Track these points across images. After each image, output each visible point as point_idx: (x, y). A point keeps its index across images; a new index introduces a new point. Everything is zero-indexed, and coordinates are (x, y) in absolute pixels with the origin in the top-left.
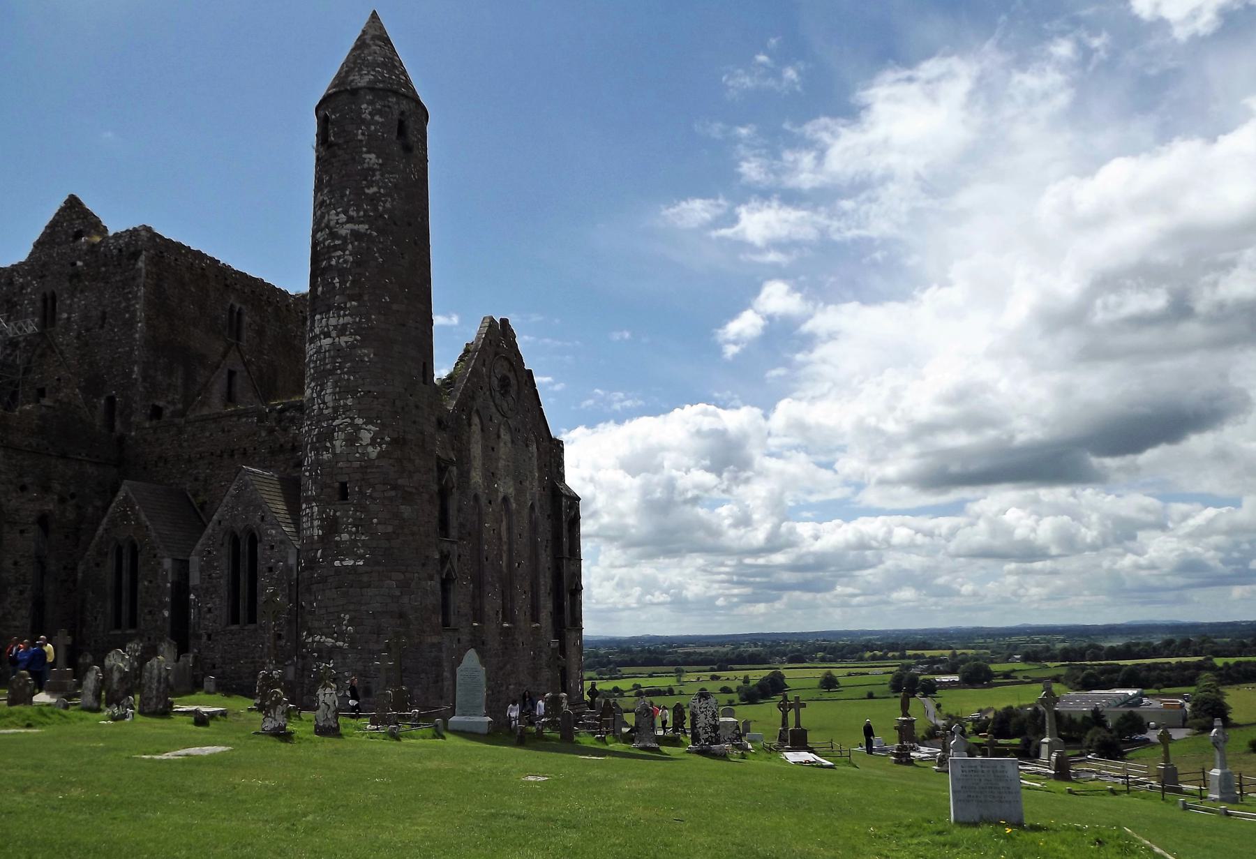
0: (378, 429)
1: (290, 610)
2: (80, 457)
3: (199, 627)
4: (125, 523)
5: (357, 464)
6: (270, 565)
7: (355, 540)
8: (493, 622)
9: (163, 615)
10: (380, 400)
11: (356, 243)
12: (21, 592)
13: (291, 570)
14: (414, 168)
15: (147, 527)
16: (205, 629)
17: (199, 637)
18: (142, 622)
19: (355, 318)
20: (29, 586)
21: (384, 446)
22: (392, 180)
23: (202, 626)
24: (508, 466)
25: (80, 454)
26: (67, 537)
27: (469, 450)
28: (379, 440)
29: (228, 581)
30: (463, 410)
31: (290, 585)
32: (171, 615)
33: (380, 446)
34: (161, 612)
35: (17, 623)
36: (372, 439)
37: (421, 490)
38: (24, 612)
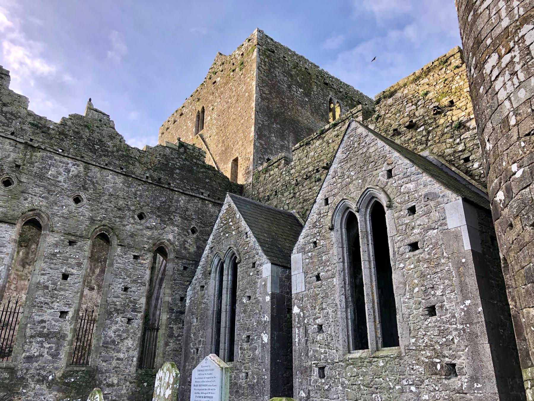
1: (468, 312)
2: (202, 196)
3: (307, 354)
4: (227, 235)
6: (412, 239)
9: (263, 341)
12: (129, 320)
13: (457, 237)
15: (246, 233)
16: (316, 359)
17: (306, 371)
18: (240, 352)
20: (139, 315)
23: (310, 353)
25: (202, 194)
26: (185, 268)
29: (344, 280)
31: (459, 265)
32: (272, 339)
34: (260, 337)
35: (121, 356)
38: (129, 343)
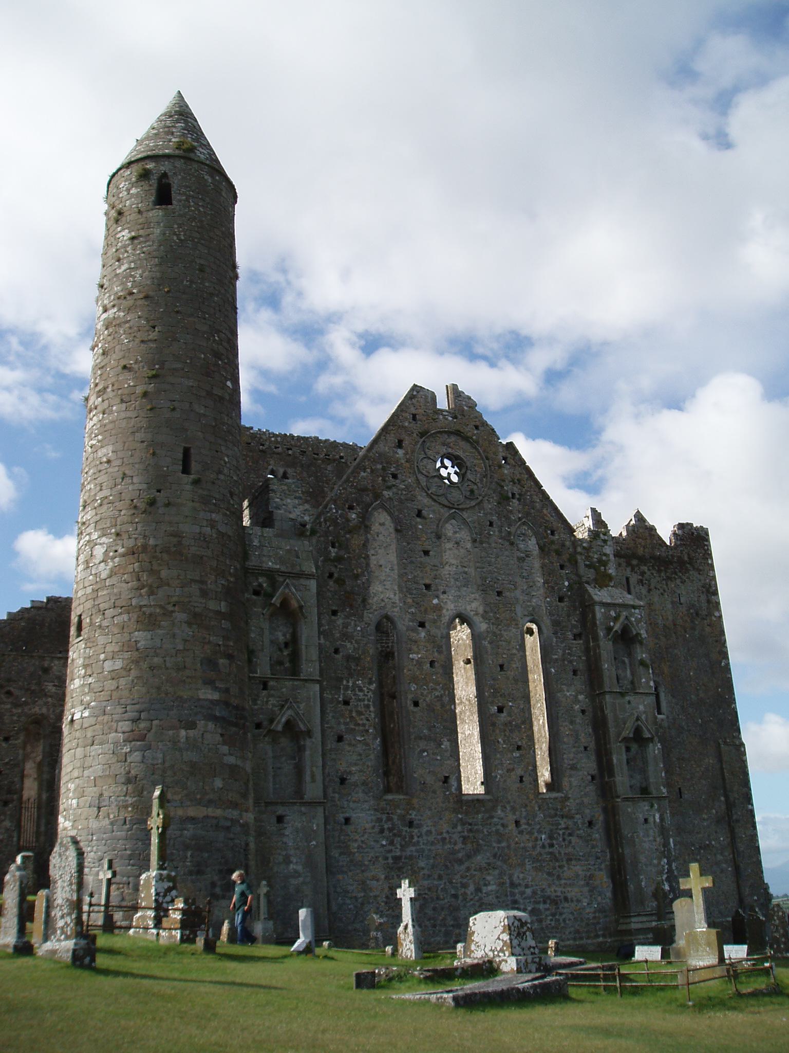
0: (111, 540)
5: (89, 590)
7: (83, 685)
8: (434, 792)
10: (117, 504)
11: (106, 332)
14: (178, 228)
19: (98, 417)
21: (117, 560)
22: (145, 249)
24: (466, 573)
27: (367, 557)
28: (111, 554)
30: (351, 508)
33: (113, 558)
36: (106, 553)
37: (170, 608)
